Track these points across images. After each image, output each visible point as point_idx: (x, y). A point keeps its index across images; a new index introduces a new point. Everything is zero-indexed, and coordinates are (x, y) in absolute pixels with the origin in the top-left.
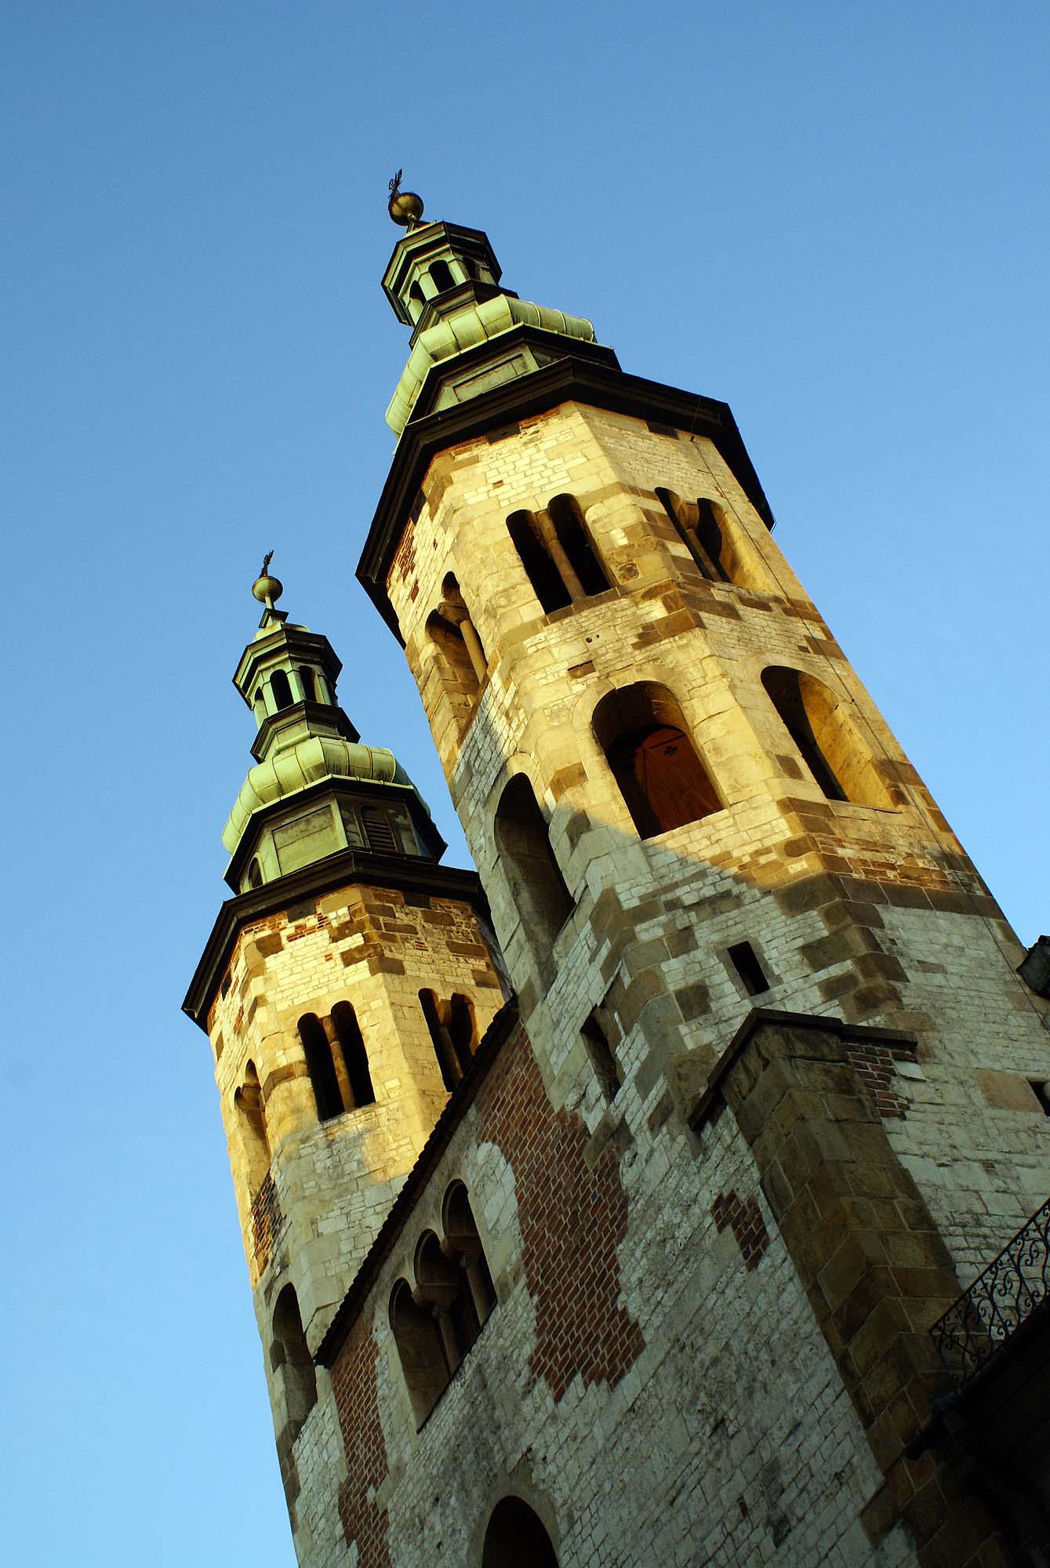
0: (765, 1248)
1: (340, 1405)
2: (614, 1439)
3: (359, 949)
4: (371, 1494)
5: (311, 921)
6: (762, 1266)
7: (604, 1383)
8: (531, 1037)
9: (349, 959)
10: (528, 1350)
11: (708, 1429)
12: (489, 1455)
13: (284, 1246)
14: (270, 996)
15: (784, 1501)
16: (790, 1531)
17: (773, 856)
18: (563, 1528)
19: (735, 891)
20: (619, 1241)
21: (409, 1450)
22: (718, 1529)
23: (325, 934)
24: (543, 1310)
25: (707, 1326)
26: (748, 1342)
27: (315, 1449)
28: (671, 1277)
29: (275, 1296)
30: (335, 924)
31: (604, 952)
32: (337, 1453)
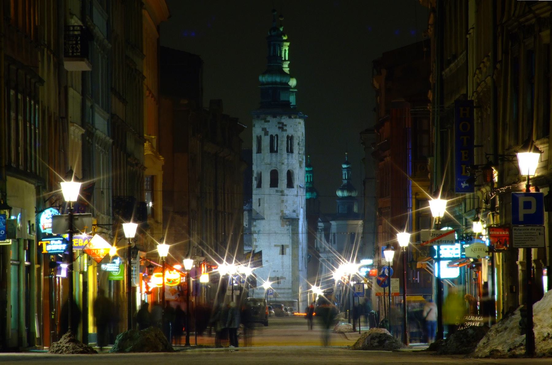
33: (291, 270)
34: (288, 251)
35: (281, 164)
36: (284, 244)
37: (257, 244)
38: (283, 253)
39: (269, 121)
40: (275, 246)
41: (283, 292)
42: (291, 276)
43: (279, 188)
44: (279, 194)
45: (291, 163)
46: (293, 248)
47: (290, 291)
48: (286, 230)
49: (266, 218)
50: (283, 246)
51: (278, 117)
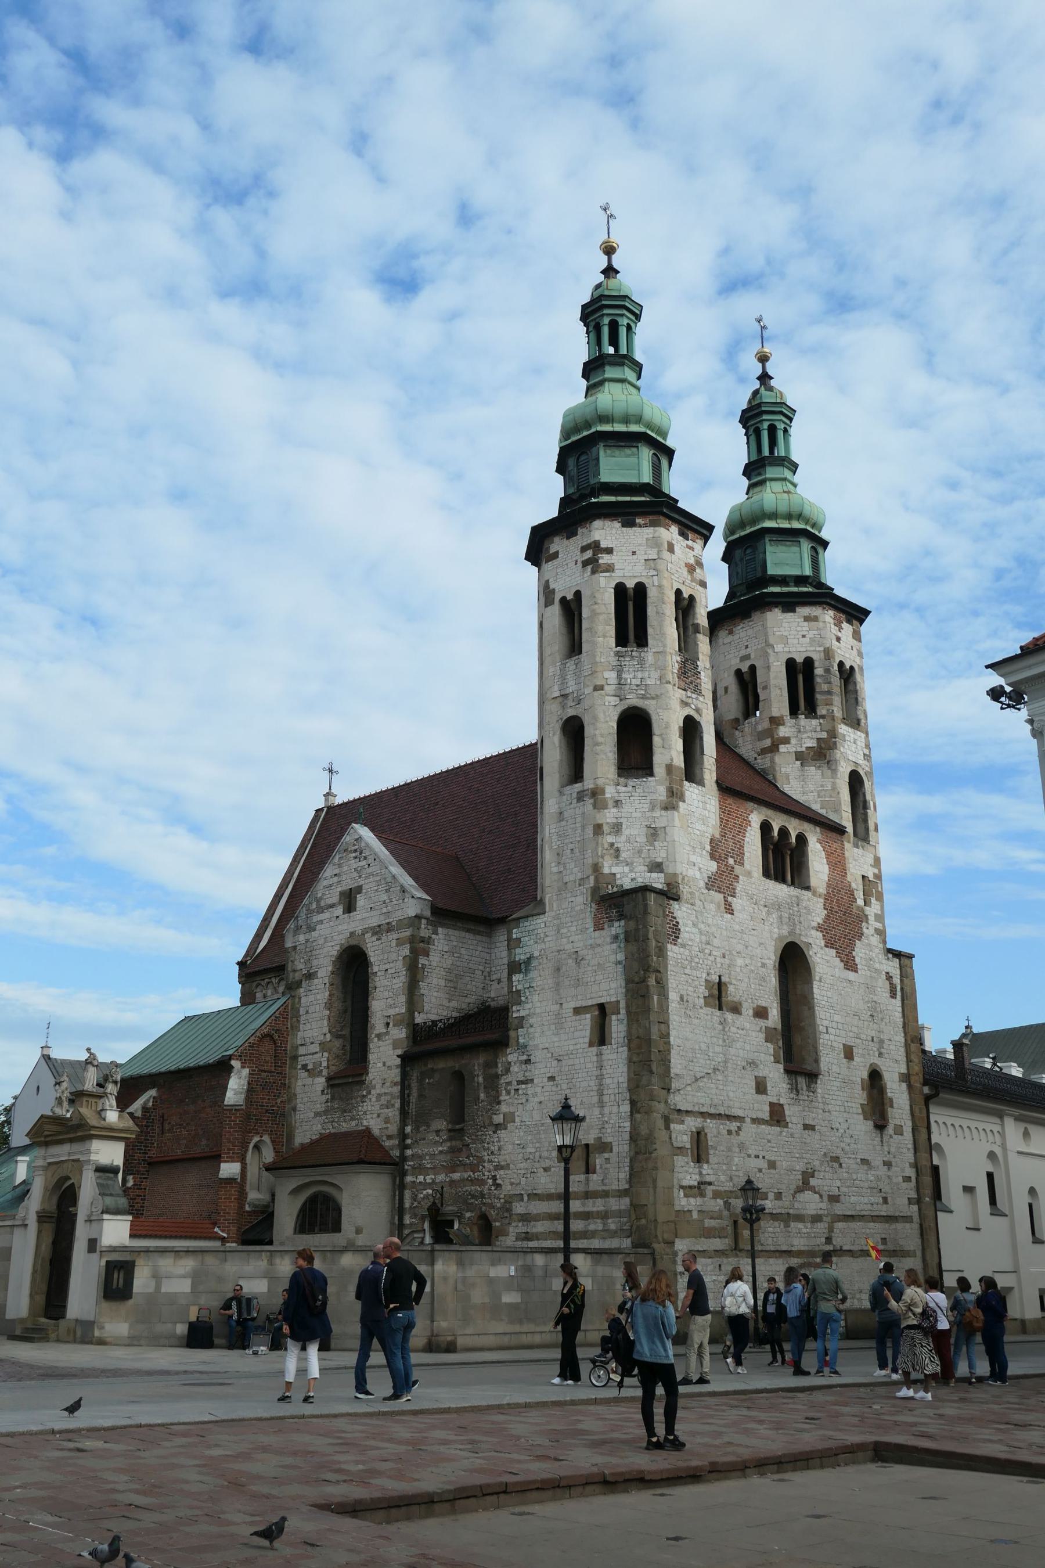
33: (626, 1108)
34: (617, 1027)
35: (591, 688)
36: (602, 1000)
37: (522, 1013)
38: (601, 1038)
39: (556, 555)
40: (577, 1011)
41: (602, 1208)
42: (627, 1136)
43: (588, 783)
44: (589, 802)
45: (634, 682)
46: (633, 1017)
47: (626, 1201)
48: (608, 940)
49: (547, 909)
50: (602, 1007)
51: (580, 530)
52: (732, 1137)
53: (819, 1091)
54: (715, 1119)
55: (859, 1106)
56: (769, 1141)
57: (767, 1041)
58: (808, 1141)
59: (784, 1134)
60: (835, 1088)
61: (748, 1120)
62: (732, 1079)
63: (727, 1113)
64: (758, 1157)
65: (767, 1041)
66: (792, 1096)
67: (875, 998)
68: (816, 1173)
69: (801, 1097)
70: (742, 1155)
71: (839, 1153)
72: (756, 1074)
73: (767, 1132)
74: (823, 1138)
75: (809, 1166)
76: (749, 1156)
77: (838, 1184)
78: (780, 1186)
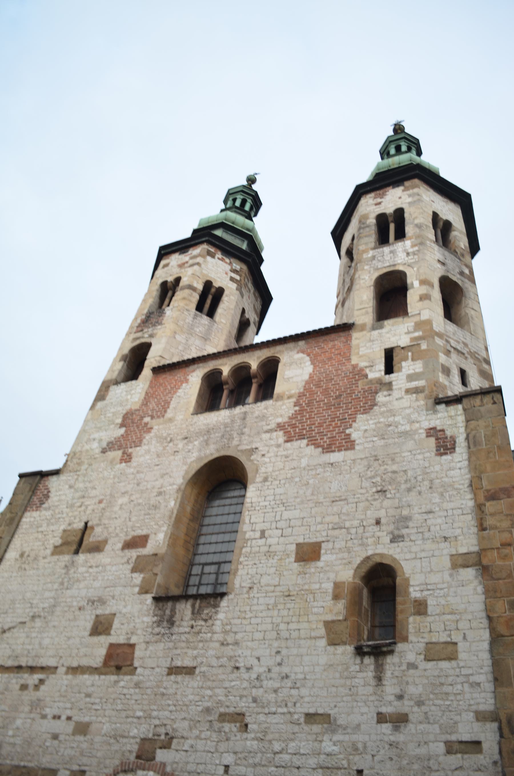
0: (450, 453)
1: (151, 386)
2: (313, 467)
3: (237, 280)
4: (147, 419)
5: (227, 260)
6: (444, 457)
7: (320, 449)
8: (353, 338)
9: (232, 279)
10: (280, 420)
11: (374, 490)
12: (231, 438)
13: (155, 331)
14: (203, 266)
15: (404, 531)
16: (403, 541)
17: (479, 357)
18: (259, 479)
19: (466, 355)
20: (362, 414)
21: (181, 417)
22: (359, 522)
23: (228, 268)
24: (296, 413)
25: (397, 460)
26: (420, 475)
27: (125, 393)
28: (386, 437)
29: (138, 342)
30: (234, 268)
31: (416, 334)
32: (137, 400)
52: (26, 692)
53: (221, 616)
54: (13, 672)
55: (321, 625)
56: (88, 695)
57: (134, 570)
58: (171, 691)
59: (122, 684)
60: (262, 608)
61: (62, 670)
62: (56, 623)
63: (30, 664)
64: (59, 717)
65: (134, 570)
66: (157, 630)
67: (395, 468)
68: (175, 741)
69: (175, 629)
70: (32, 716)
71: (243, 705)
72: (99, 612)
73: (89, 683)
74: (209, 684)
75: (162, 730)
76: (44, 717)
77: (229, 759)
78: (85, 760)
